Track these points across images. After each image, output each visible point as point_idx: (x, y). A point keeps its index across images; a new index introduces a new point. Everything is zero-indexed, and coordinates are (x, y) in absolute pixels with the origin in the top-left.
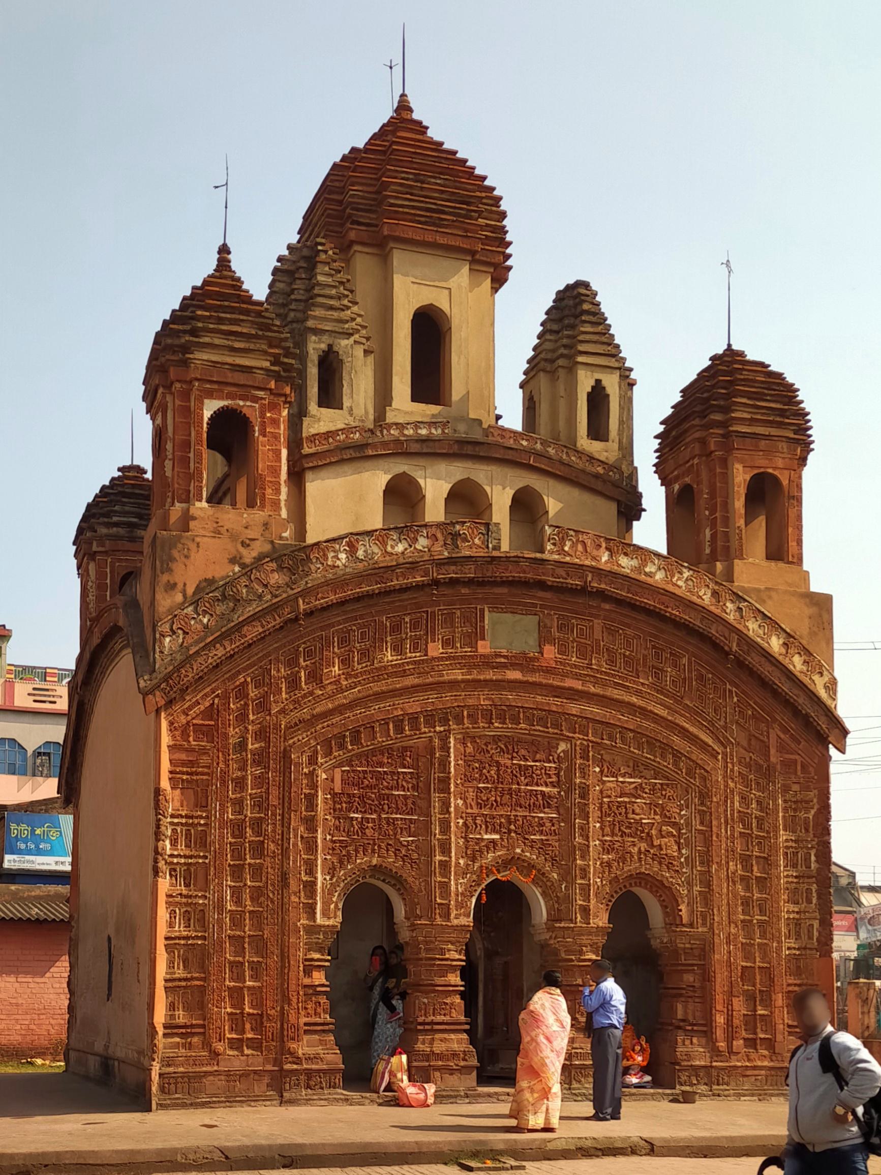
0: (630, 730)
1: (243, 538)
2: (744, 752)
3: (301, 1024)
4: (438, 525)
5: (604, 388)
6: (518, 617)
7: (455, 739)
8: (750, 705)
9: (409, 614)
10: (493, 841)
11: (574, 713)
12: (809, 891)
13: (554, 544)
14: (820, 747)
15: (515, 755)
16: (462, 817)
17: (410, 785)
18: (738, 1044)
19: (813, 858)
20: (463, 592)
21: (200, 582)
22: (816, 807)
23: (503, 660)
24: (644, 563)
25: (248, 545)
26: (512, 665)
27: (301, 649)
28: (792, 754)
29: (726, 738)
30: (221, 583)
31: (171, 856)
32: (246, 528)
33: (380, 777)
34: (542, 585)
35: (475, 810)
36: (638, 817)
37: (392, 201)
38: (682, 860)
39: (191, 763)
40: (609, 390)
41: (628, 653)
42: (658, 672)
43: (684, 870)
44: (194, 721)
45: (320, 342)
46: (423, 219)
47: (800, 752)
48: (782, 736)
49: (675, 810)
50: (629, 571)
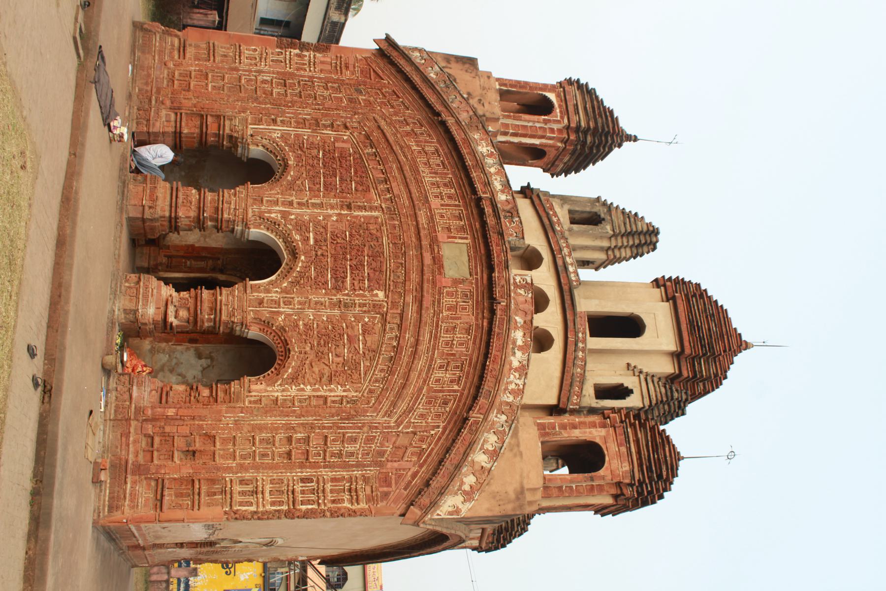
0: (399, 342)
6: (467, 265)
7: (377, 218)
8: (430, 445)
9: (456, 192)
10: (308, 238)
11: (406, 299)
12: (281, 503)
13: (520, 282)
16: (324, 220)
17: (343, 188)
18: (149, 429)
19: (310, 507)
20: (477, 224)
21: (453, 76)
22: (353, 507)
23: (436, 251)
25: (480, 103)
26: (434, 258)
28: (396, 484)
29: (402, 423)
31: (291, 52)
32: (489, 103)
33: (348, 170)
34: (491, 269)
35: (329, 230)
39: (347, 68)
40: (628, 399)
42: (444, 367)
44: (372, 70)
45: (605, 214)
46: (691, 317)
47: (398, 491)
48: (410, 473)
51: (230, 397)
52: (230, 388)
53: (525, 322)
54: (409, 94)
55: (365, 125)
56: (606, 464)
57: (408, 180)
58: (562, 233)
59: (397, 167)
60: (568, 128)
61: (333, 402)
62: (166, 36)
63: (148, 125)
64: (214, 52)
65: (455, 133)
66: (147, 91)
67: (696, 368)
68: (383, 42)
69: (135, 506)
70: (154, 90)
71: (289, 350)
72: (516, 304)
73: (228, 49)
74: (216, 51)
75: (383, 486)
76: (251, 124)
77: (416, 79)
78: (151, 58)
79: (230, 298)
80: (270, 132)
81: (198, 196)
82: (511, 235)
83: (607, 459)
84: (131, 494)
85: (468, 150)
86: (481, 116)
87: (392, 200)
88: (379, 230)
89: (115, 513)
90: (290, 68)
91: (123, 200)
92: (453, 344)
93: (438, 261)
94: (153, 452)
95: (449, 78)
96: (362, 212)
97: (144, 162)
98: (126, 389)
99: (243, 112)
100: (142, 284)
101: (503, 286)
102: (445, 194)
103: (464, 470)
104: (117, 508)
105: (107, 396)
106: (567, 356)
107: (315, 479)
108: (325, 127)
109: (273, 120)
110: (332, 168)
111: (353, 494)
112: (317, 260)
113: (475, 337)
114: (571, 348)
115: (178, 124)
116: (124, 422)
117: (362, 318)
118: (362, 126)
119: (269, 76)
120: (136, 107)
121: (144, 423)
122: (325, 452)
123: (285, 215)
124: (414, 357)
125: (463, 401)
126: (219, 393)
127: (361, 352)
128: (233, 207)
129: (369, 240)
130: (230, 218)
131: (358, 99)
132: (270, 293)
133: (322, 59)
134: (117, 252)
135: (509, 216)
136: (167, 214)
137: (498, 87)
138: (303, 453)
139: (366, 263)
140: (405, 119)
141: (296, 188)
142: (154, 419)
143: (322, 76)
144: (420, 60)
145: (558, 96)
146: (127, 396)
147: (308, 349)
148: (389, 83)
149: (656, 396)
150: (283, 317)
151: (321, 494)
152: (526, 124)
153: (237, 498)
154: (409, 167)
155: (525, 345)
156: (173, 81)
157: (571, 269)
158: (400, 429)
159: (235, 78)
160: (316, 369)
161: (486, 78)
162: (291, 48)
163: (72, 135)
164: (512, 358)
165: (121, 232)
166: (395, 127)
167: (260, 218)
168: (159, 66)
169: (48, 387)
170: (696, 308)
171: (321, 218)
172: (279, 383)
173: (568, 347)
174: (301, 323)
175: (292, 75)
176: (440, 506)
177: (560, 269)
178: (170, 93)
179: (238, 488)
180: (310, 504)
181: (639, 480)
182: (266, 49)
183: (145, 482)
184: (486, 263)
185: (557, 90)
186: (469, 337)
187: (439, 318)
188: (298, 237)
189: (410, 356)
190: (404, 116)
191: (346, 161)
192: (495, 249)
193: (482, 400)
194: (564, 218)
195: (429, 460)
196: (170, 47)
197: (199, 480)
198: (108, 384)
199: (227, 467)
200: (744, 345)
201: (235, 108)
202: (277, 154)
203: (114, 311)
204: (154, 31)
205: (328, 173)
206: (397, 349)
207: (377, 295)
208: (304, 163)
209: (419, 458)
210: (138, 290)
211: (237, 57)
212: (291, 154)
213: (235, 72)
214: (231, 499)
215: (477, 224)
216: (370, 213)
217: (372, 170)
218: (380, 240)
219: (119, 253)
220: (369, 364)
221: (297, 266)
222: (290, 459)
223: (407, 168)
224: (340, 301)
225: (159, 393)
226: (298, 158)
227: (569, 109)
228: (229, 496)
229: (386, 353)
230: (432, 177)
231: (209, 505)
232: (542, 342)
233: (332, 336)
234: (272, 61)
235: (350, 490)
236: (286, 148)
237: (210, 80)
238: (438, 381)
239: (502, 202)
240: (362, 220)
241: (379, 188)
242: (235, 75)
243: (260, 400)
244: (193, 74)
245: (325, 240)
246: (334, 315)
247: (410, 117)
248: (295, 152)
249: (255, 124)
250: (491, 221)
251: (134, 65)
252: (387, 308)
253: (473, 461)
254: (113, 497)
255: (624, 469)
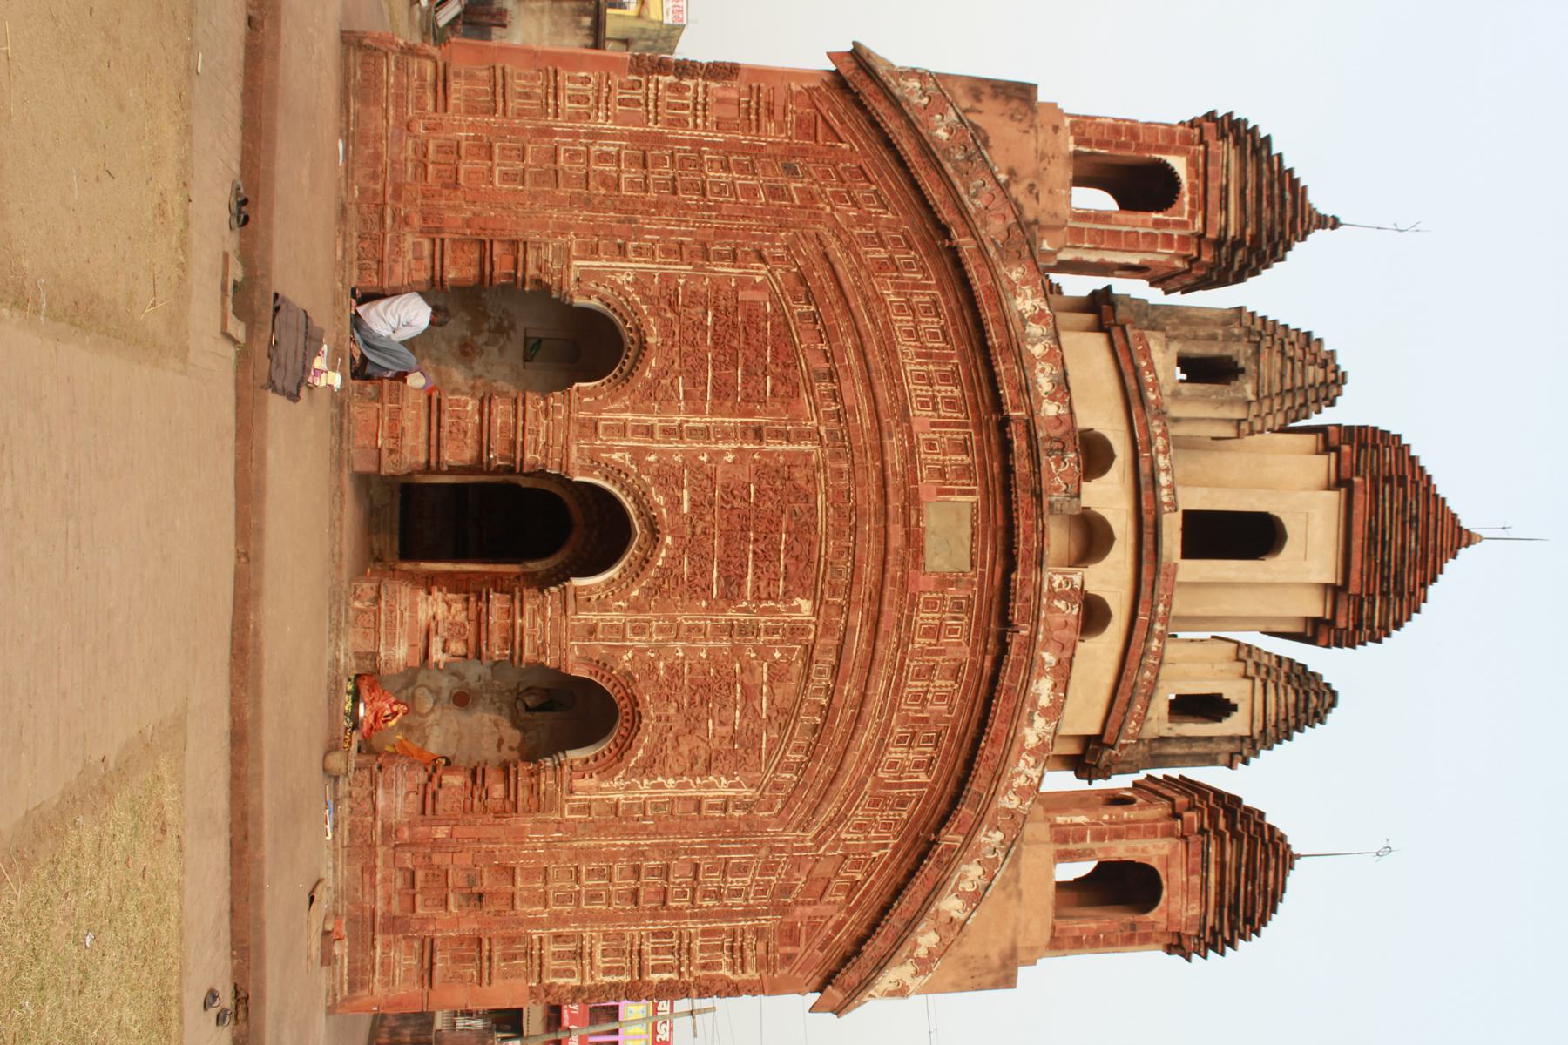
0: (831, 699)
1: (1039, 187)
2: (807, 869)
3: (442, 236)
4: (1073, 428)
5: (1228, 715)
6: (967, 543)
7: (809, 454)
8: (869, 876)
10: (679, 501)
11: (851, 618)
12: (619, 971)
13: (1060, 585)
14: (817, 979)
15: (793, 536)
16: (709, 461)
17: (750, 391)
19: (666, 976)
20: (995, 464)
21: (984, 131)
22: (736, 978)
23: (913, 521)
24: (1045, 712)
25: (1031, 192)
26: (908, 535)
27: (913, 253)
28: (807, 940)
29: (825, 841)
30: (984, 152)
31: (657, 82)
32: (1050, 192)
34: (1010, 566)
35: (719, 481)
36: (716, 713)
37: (1387, 488)
38: (660, 779)
39: (771, 113)
41: (929, 696)
42: (909, 741)
43: (646, 782)
45: (1247, 359)
46: (1373, 523)
47: (809, 951)
48: (831, 924)
49: (727, 768)
50: (1033, 690)
51: (539, 800)
52: (539, 784)
53: (1059, 662)
54: (891, 174)
55: (799, 253)
56: (1162, 904)
57: (874, 374)
58: (1158, 404)
59: (855, 346)
60: (1201, 237)
61: (712, 807)
62: (410, 58)
63: (380, 273)
64: (504, 86)
65: (973, 274)
66: (375, 193)
67: (1365, 613)
68: (847, 59)
69: (388, 982)
70: (389, 190)
71: (640, 717)
72: (1048, 630)
73: (533, 78)
74: (508, 88)
75: (783, 944)
76: (577, 258)
77: (907, 147)
78: (380, 114)
79: (539, 620)
80: (613, 273)
81: (477, 417)
82: (1057, 489)
83: (1165, 894)
84: (382, 964)
85: (995, 313)
86: (1029, 224)
87: (839, 416)
88: (812, 479)
89: (360, 993)
90: (656, 122)
91: (342, 442)
92: (925, 699)
93: (914, 541)
94: (414, 896)
95: (974, 140)
96: (781, 444)
97: (376, 343)
98: (366, 793)
99: (562, 234)
100: (383, 604)
101: (1028, 600)
102: (943, 398)
103: (922, 926)
104: (363, 986)
105: (335, 810)
106: (1131, 648)
107: (675, 933)
108: (721, 256)
109: (619, 246)
110: (731, 347)
111: (737, 955)
112: (692, 544)
113: (967, 685)
114: (1140, 633)
115: (438, 263)
116: (366, 849)
117: (770, 652)
118: (793, 257)
119: (613, 145)
120: (355, 234)
121: (399, 849)
122: (694, 891)
123: (638, 454)
124: (855, 728)
125: (933, 802)
126: (520, 791)
127: (764, 716)
128: (542, 440)
129: (792, 499)
130: (537, 461)
131: (788, 189)
132: (607, 611)
133: (721, 94)
134: (337, 547)
135: (1058, 449)
136: (422, 459)
137: (1072, 147)
138: (657, 893)
139: (782, 547)
140: (878, 234)
141: (661, 395)
142: (413, 844)
143: (719, 138)
144: (921, 98)
145: (1192, 163)
146: (368, 806)
147: (672, 711)
148: (852, 149)
149: (1277, 714)
150: (630, 655)
151: (684, 957)
152: (1118, 228)
153: (552, 964)
154: (878, 343)
155: (1053, 706)
156: (426, 166)
157: (1164, 479)
158: (820, 852)
159: (546, 151)
160: (684, 749)
161: (1049, 128)
162: (659, 73)
163: (237, 512)
164: (1027, 731)
165: (342, 509)
166: (857, 255)
167: (593, 461)
168: (397, 131)
169: (242, 995)
170: (1387, 505)
171: (705, 458)
172: (621, 774)
173: (1135, 633)
174: (662, 664)
175: (660, 139)
176: (874, 985)
177: (1143, 480)
178: (420, 196)
179: (551, 948)
180: (665, 972)
181: (1213, 928)
182: (608, 78)
183: (403, 943)
184: (1004, 544)
185: (1192, 148)
186: (956, 686)
187: (906, 653)
188: (660, 500)
189: (850, 722)
190: (876, 227)
191: (758, 331)
192: (1022, 524)
193: (965, 811)
194: (1166, 370)
195: (865, 901)
196: (416, 84)
197: (490, 939)
198: (335, 790)
199: (535, 919)
200: (1464, 541)
201: (546, 226)
202: (625, 316)
203: (338, 661)
204: (383, 48)
205: (722, 358)
206: (827, 712)
207: (798, 609)
208: (677, 338)
209: (849, 897)
210: (377, 615)
211: (551, 101)
212: (652, 320)
213: (546, 140)
214: (541, 965)
215: (995, 464)
216: (796, 447)
217: (807, 352)
218: (811, 500)
219: (340, 549)
220: (776, 736)
221: (658, 556)
222: (636, 904)
223: (873, 345)
224: (732, 625)
225: (421, 793)
226: (666, 327)
227: (1210, 198)
228: (537, 962)
229: (809, 718)
230: (920, 364)
231: (505, 976)
232: (1093, 615)
233: (716, 687)
234: (621, 102)
235: (731, 948)
236: (644, 307)
237: (497, 160)
238: (893, 765)
239: (1048, 420)
240: (781, 459)
241: (817, 394)
242: (546, 144)
243: (589, 807)
244: (464, 144)
245: (711, 504)
246: (721, 648)
247: (889, 229)
248: (659, 315)
249: (585, 259)
250: (1021, 466)
251: (347, 137)
252: (816, 635)
253: (937, 911)
254: (355, 969)
255: (1191, 913)
